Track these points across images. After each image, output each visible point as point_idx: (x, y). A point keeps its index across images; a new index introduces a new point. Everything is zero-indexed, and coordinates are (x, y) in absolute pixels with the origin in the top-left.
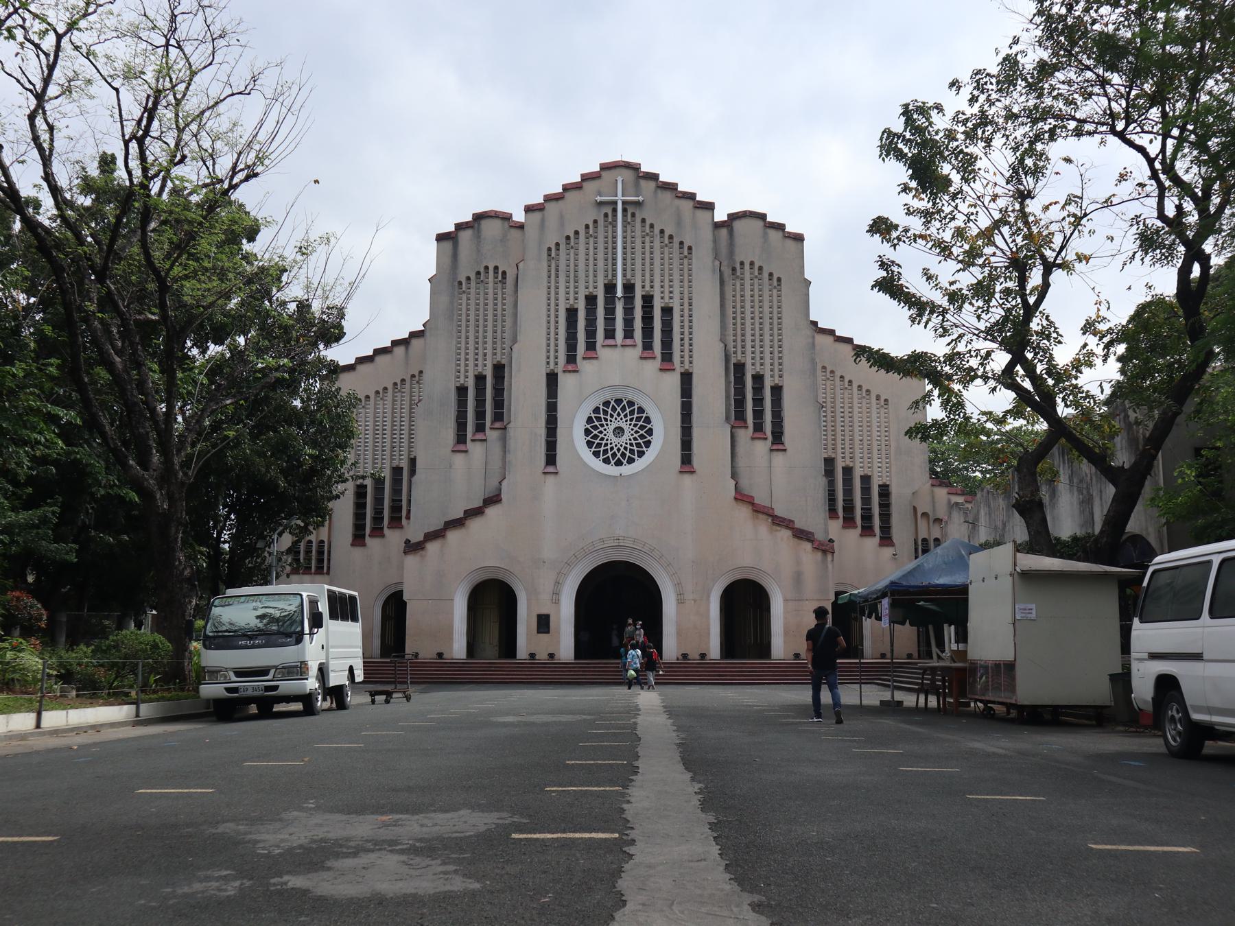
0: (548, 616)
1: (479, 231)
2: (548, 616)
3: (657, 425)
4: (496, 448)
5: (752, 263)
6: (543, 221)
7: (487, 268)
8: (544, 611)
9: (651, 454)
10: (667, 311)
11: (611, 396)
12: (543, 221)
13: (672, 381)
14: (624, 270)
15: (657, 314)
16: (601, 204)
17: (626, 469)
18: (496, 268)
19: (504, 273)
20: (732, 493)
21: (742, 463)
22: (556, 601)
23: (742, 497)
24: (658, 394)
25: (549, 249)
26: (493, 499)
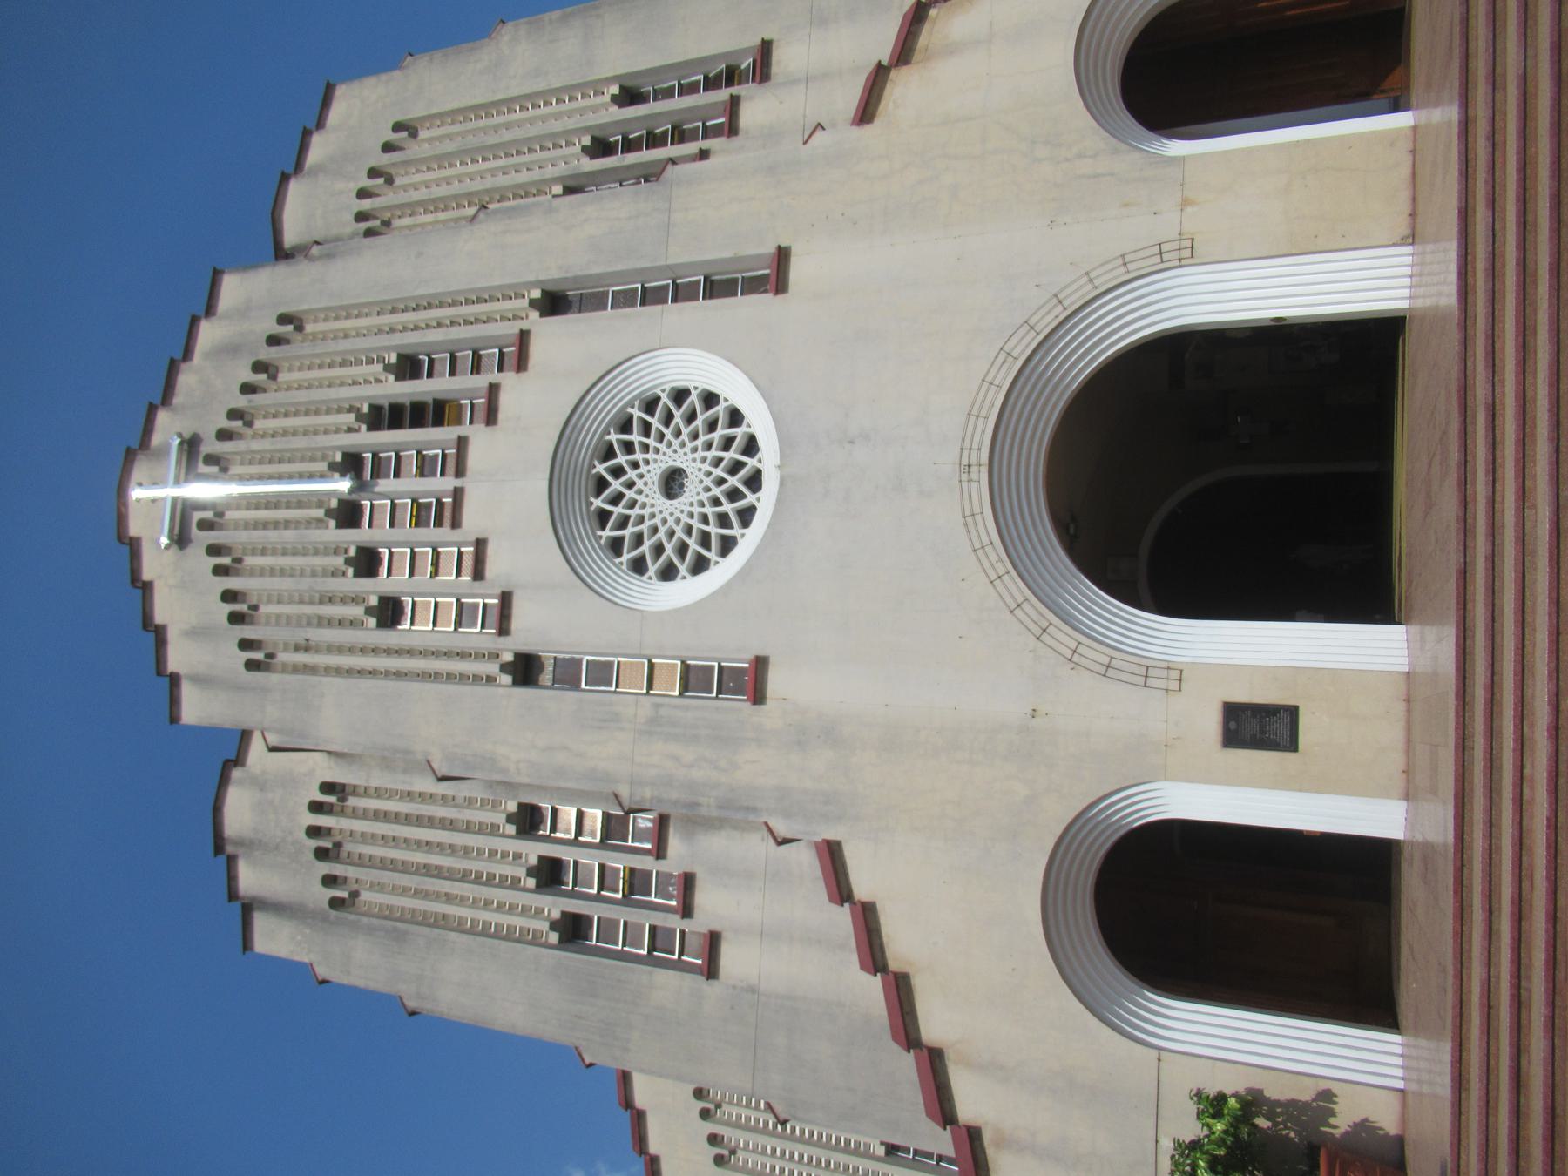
0: (1232, 712)
1: (240, 843)
2: (1232, 712)
4: (716, 844)
5: (363, 194)
6: (198, 680)
7: (314, 832)
8: (1212, 724)
9: (736, 389)
10: (408, 367)
12: (198, 680)
14: (311, 477)
16: (181, 539)
18: (316, 807)
19: (327, 788)
22: (1177, 676)
25: (252, 665)
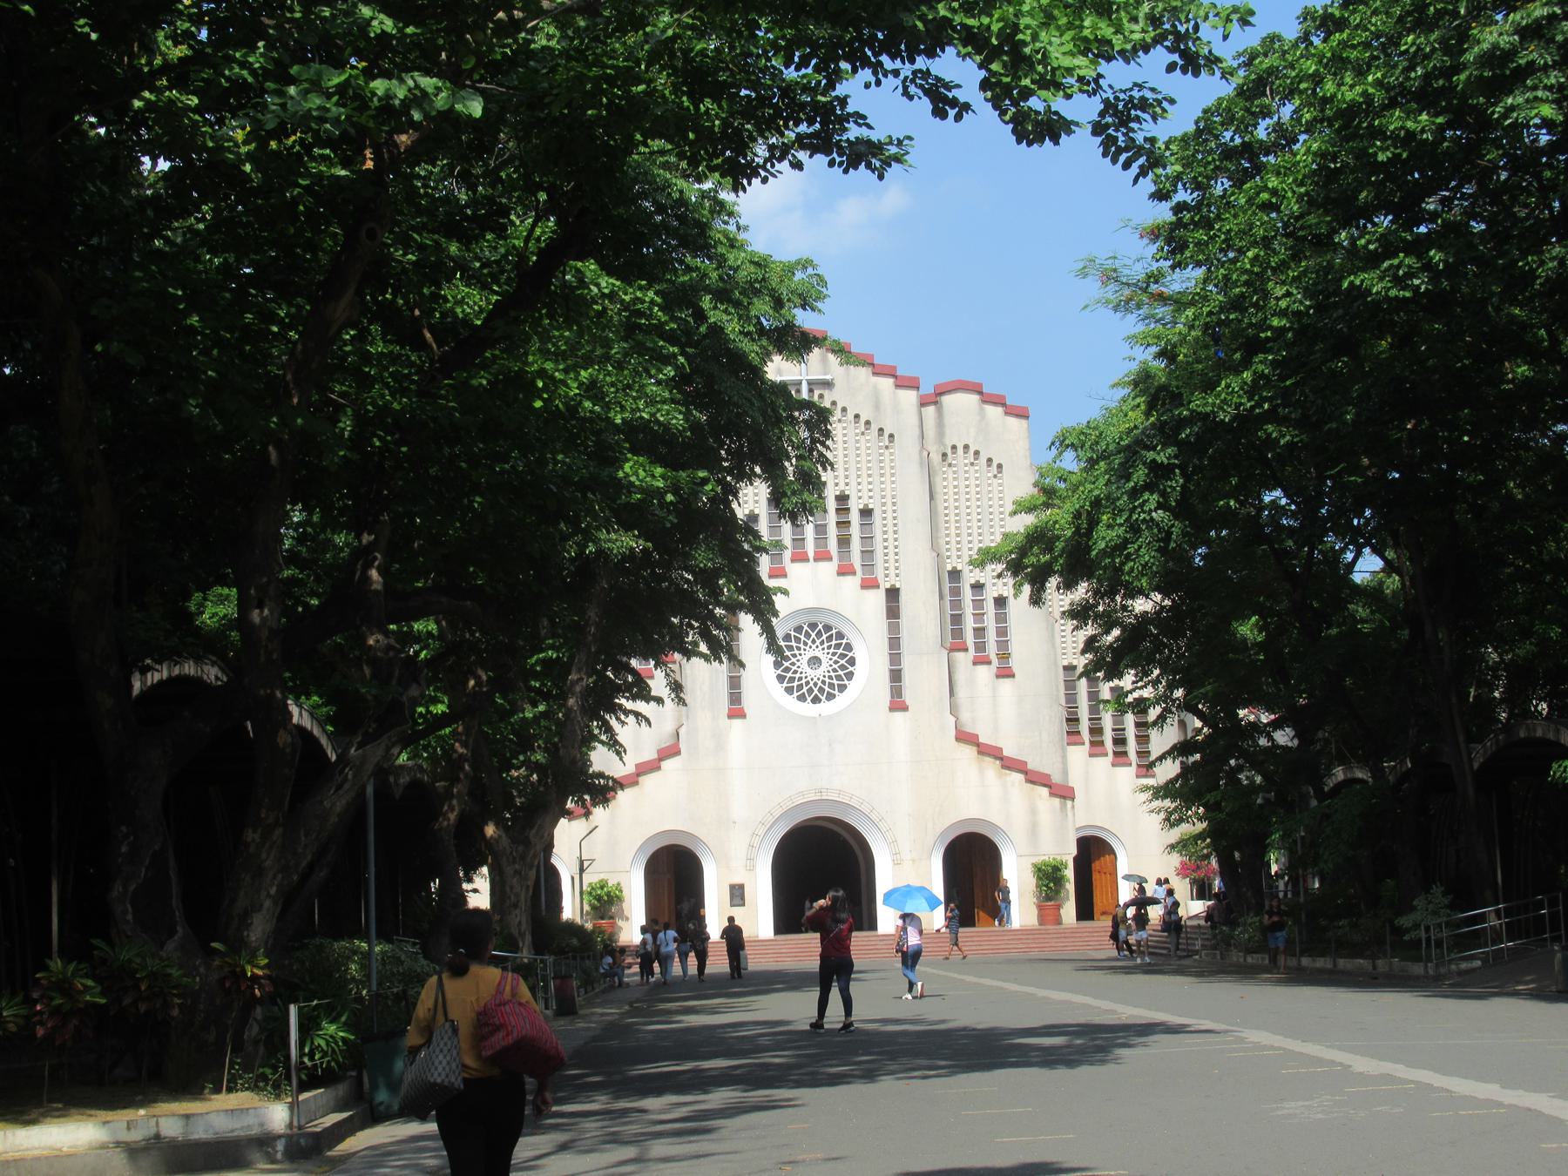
0: (742, 887)
2: (742, 887)
3: (859, 652)
5: (966, 447)
8: (737, 880)
9: (854, 687)
11: (804, 621)
13: (877, 598)
15: (854, 517)
17: (825, 707)
20: (953, 733)
21: (962, 693)
22: (751, 869)
23: (964, 737)
24: (862, 612)
26: (670, 751)
